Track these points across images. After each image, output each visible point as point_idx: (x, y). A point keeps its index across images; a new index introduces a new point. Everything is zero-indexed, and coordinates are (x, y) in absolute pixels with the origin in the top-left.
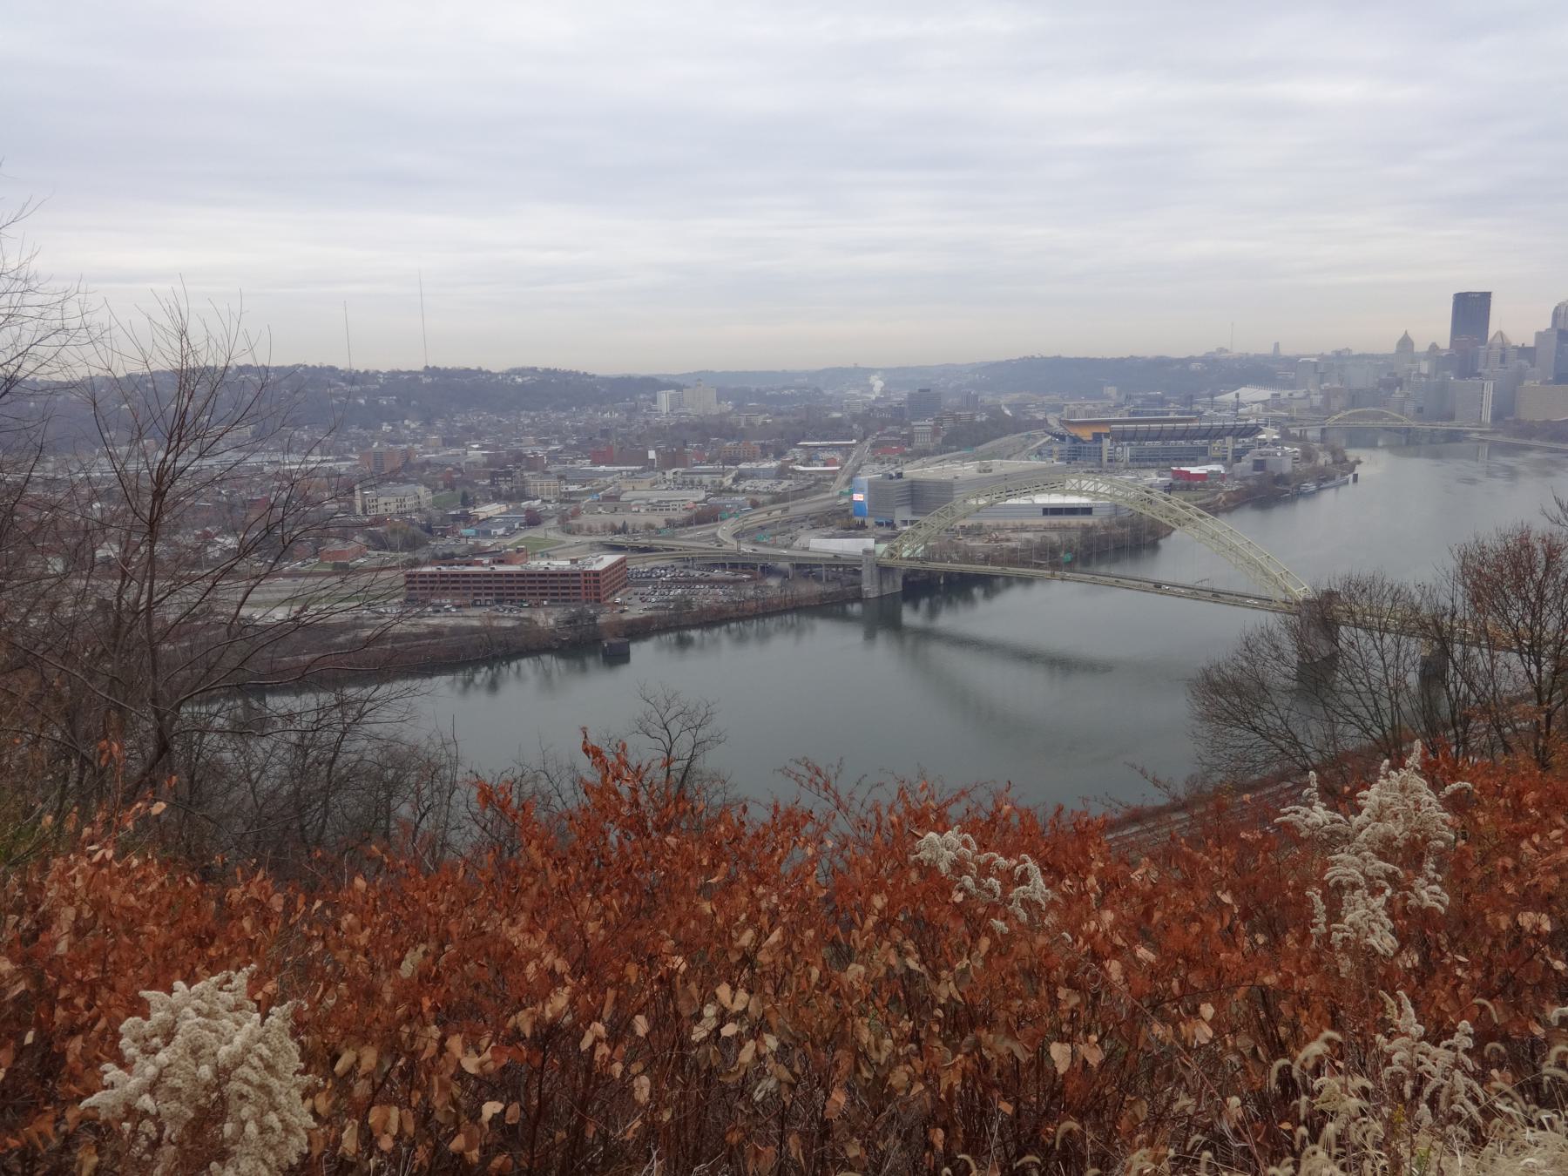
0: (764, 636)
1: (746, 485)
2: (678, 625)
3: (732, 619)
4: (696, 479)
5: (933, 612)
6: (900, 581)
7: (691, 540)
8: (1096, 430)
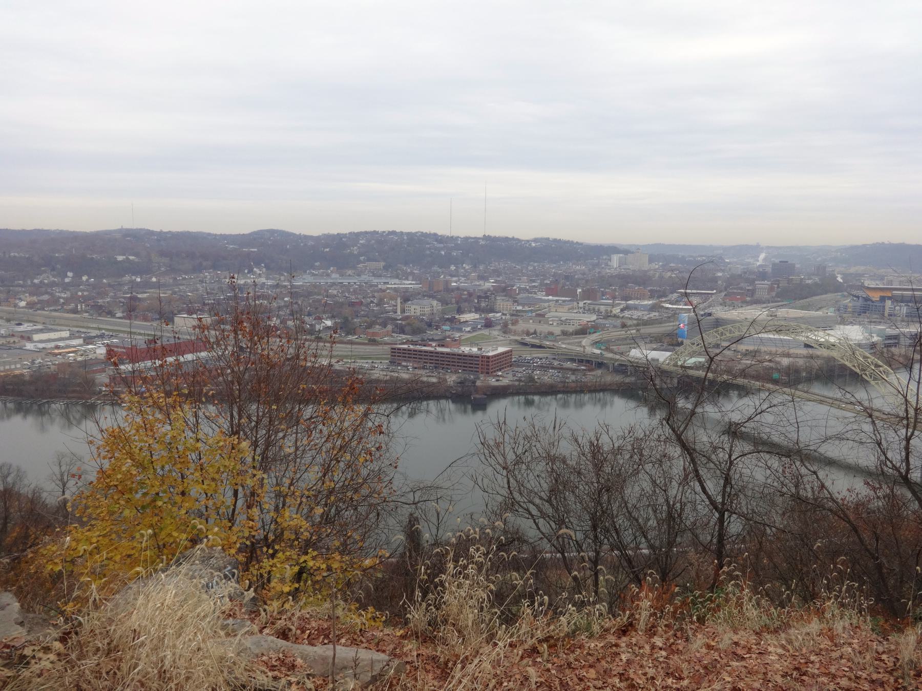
0: (580, 405)
1: (627, 314)
2: (528, 391)
3: (559, 392)
4: (597, 308)
6: (676, 381)
7: (568, 344)
8: (883, 294)
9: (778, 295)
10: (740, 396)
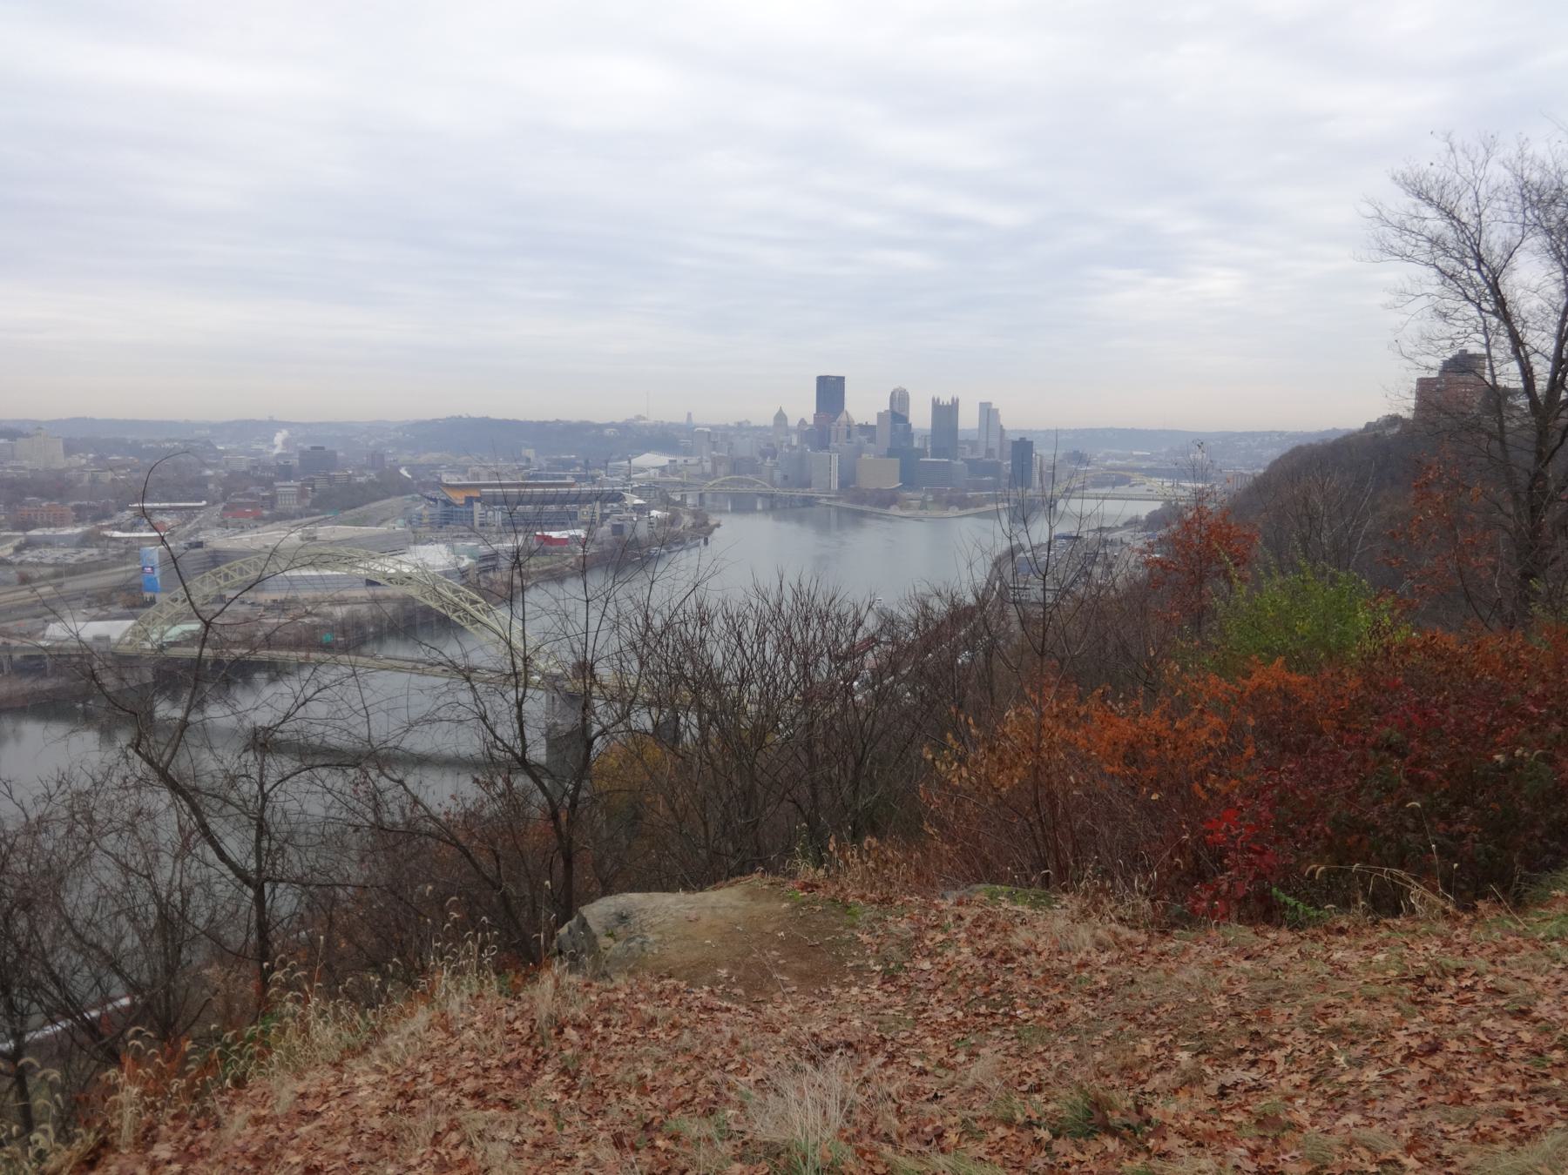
1: (29, 556)
5: (198, 704)
9: (315, 504)
10: (272, 680)
